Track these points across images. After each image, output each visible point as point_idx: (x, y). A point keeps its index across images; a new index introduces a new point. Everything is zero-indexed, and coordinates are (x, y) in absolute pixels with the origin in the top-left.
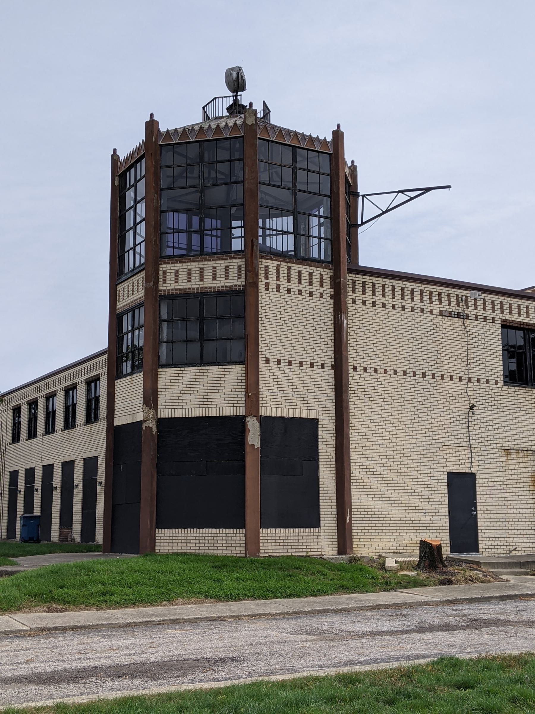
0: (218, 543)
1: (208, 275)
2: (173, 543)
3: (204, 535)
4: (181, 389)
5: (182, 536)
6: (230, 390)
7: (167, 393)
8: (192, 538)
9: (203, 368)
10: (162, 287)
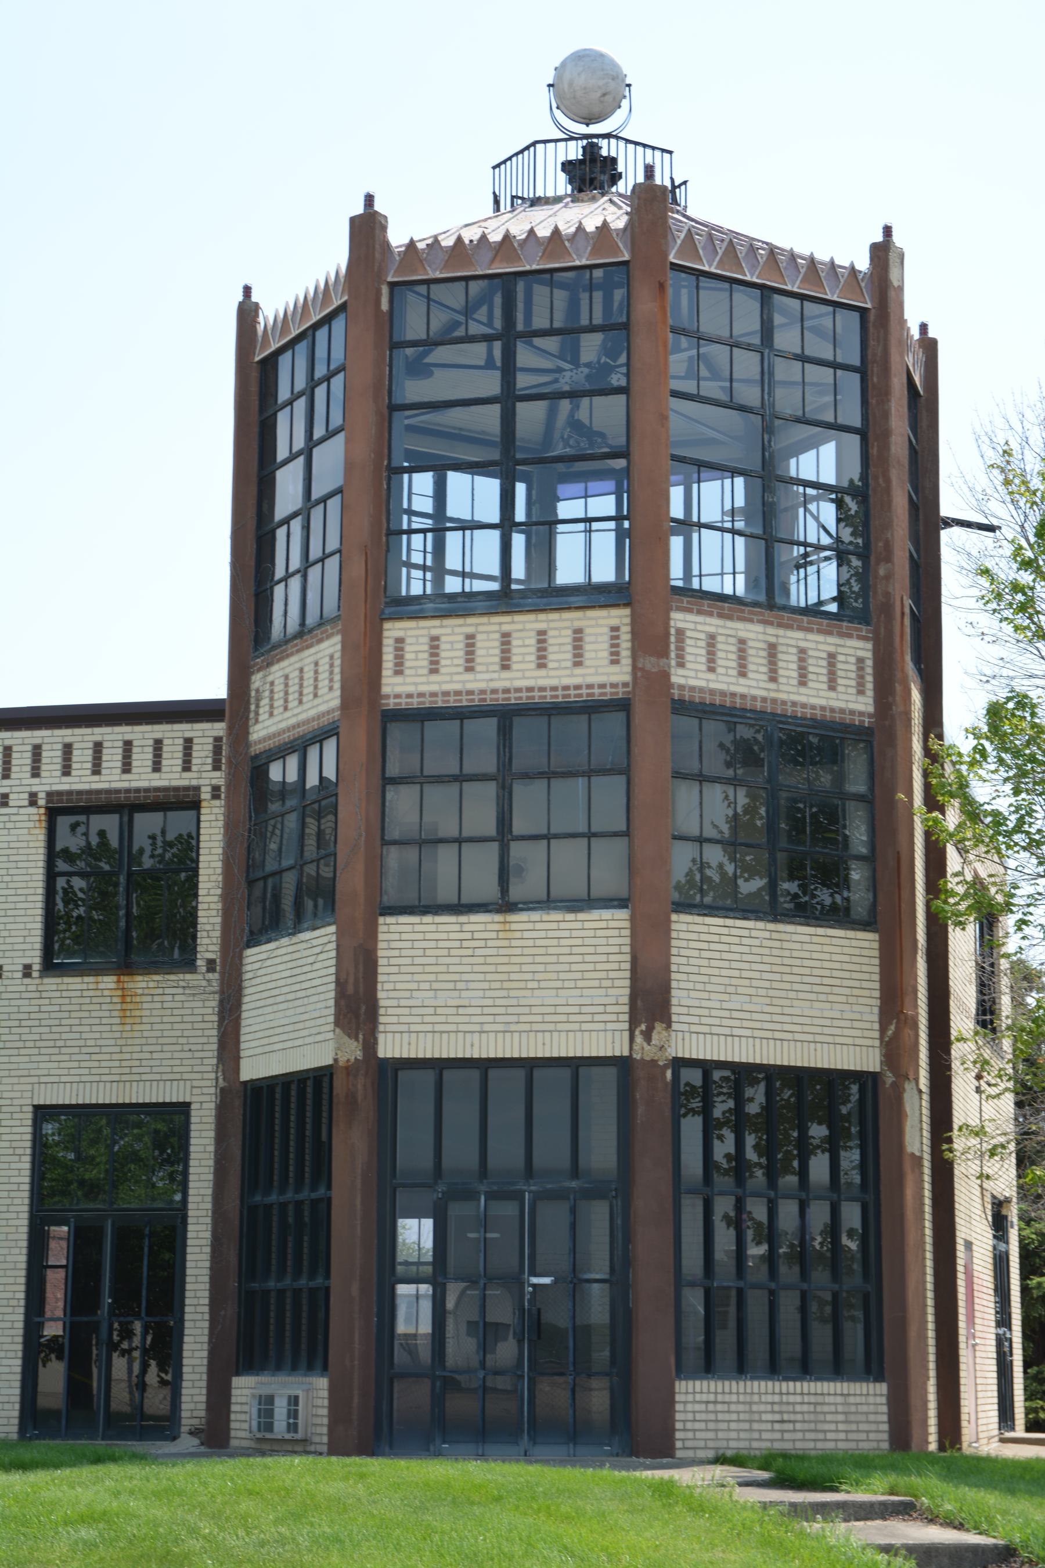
0: (825, 1422)
1: (788, 669)
2: (717, 1421)
3: (792, 1399)
4: (727, 981)
5: (738, 1402)
6: (843, 999)
7: (690, 986)
8: (762, 1408)
9: (781, 927)
10: (678, 677)
